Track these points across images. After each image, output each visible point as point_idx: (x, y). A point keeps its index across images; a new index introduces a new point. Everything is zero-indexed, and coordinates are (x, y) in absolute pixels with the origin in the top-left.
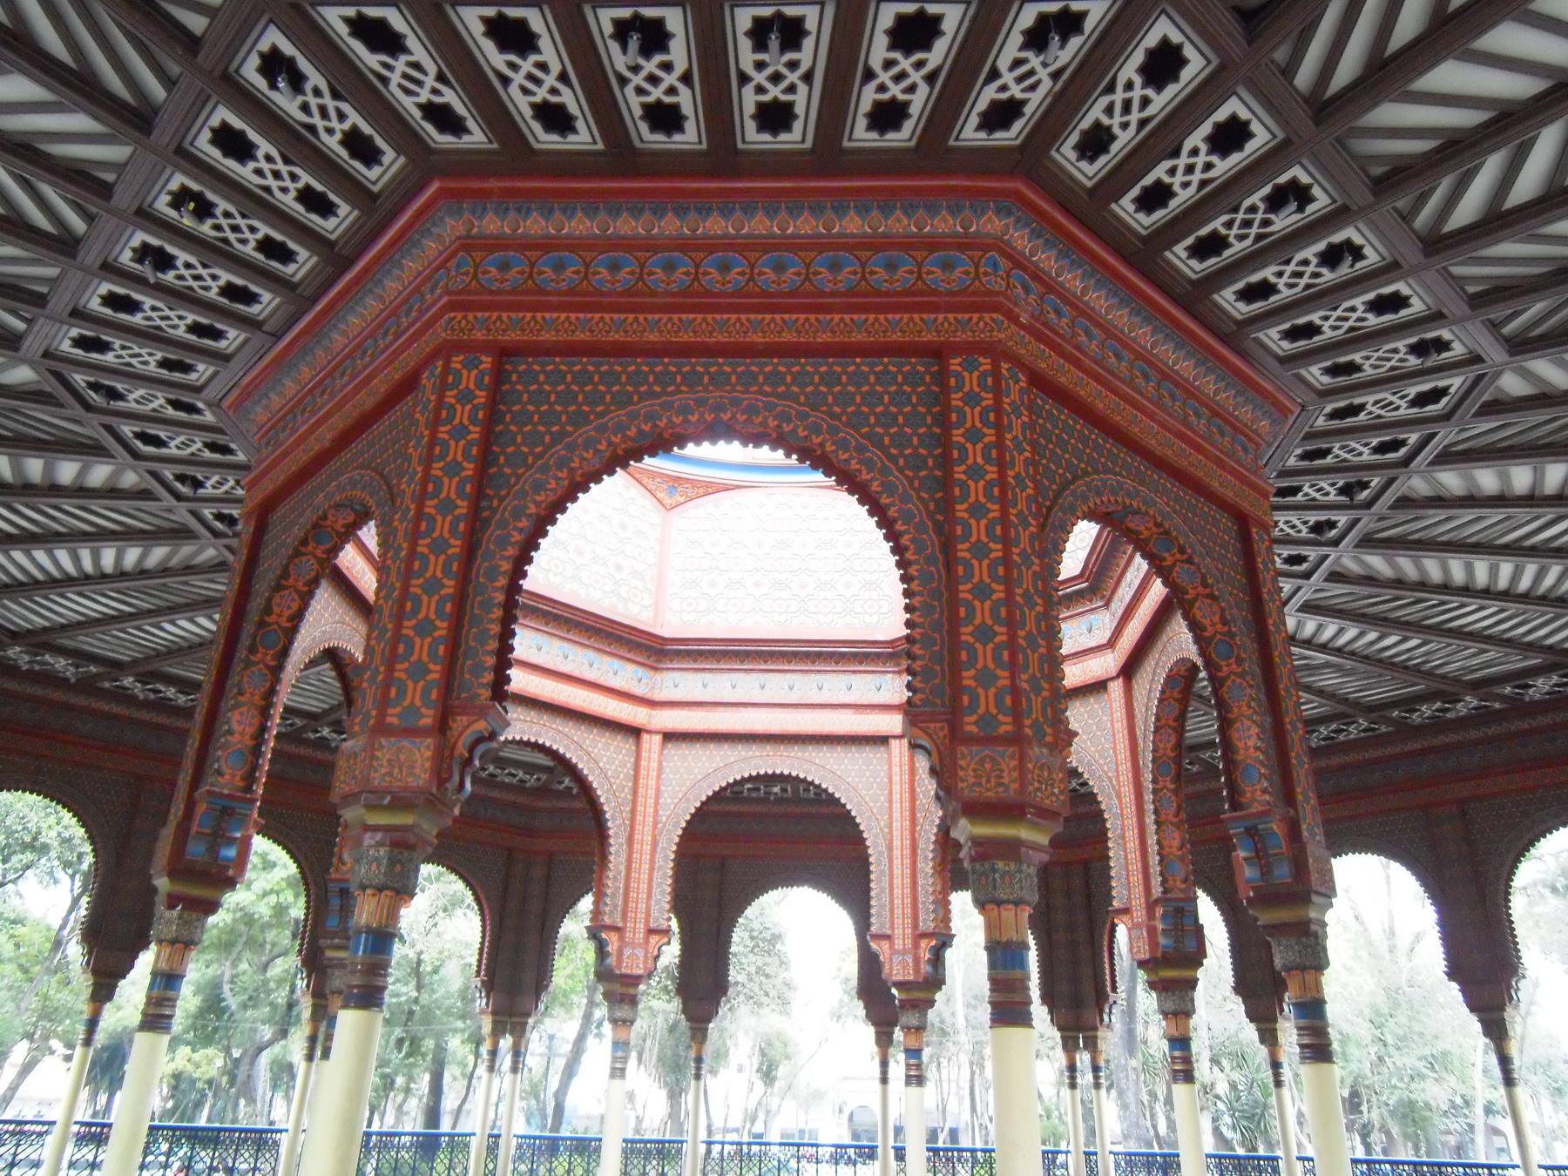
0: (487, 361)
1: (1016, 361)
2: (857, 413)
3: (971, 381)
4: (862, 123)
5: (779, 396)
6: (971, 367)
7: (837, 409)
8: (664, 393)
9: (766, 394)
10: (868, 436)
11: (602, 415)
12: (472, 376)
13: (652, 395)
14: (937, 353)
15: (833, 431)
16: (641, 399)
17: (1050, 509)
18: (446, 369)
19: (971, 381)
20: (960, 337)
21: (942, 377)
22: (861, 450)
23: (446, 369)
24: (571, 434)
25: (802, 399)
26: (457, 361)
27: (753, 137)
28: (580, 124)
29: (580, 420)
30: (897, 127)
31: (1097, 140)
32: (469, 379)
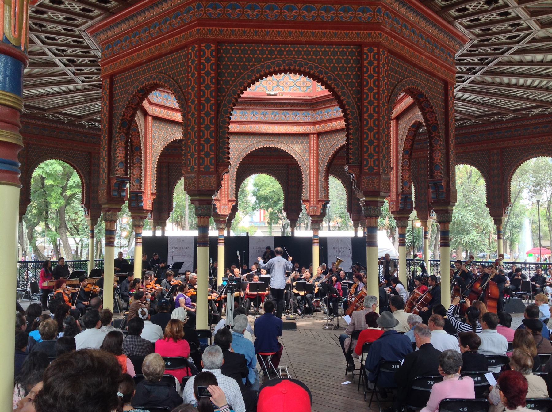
1: (385, 48)
2: (334, 66)
3: (371, 56)
6: (371, 51)
7: (327, 65)
8: (272, 58)
9: (305, 59)
10: (336, 75)
11: (252, 66)
14: (360, 46)
15: (326, 73)
17: (390, 96)
19: (371, 56)
20: (368, 40)
21: (361, 54)
22: (335, 80)
23: (200, 50)
24: (242, 73)
25: (316, 61)
29: (245, 68)
32: (208, 53)
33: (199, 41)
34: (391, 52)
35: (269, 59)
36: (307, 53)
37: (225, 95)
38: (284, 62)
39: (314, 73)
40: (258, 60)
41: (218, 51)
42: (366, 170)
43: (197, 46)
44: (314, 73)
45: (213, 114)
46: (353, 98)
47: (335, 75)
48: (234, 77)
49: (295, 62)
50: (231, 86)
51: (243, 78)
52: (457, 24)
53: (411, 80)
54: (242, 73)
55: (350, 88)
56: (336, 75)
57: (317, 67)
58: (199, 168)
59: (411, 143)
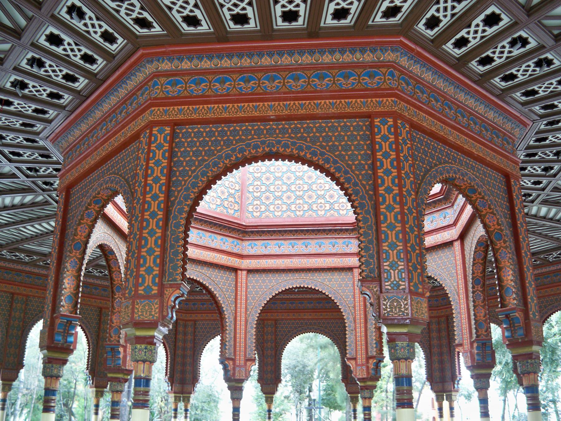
0: (168, 130)
2: (334, 145)
3: (384, 130)
4: (329, 17)
5: (298, 139)
6: (384, 123)
9: (292, 138)
12: (161, 136)
13: (241, 140)
16: (237, 142)
18: (151, 134)
19: (384, 130)
22: (335, 162)
24: (205, 160)
26: (155, 130)
27: (280, 24)
28: (203, 22)
30: (345, 17)
31: (433, 23)
32: (160, 138)
33: (151, 125)
34: (414, 126)
35: (243, 141)
36: (296, 130)
37: (181, 189)
38: (263, 143)
39: (305, 155)
40: (228, 143)
41: (173, 134)
42: (387, 285)
43: (148, 131)
44: (305, 155)
45: (160, 215)
46: (363, 185)
47: (335, 156)
48: (195, 166)
49: (279, 142)
50: (190, 177)
51: (207, 166)
52: (508, 99)
53: (451, 168)
54: (205, 160)
55: (357, 173)
56: (340, 156)
57: (308, 148)
58: (136, 290)
59: (481, 268)
